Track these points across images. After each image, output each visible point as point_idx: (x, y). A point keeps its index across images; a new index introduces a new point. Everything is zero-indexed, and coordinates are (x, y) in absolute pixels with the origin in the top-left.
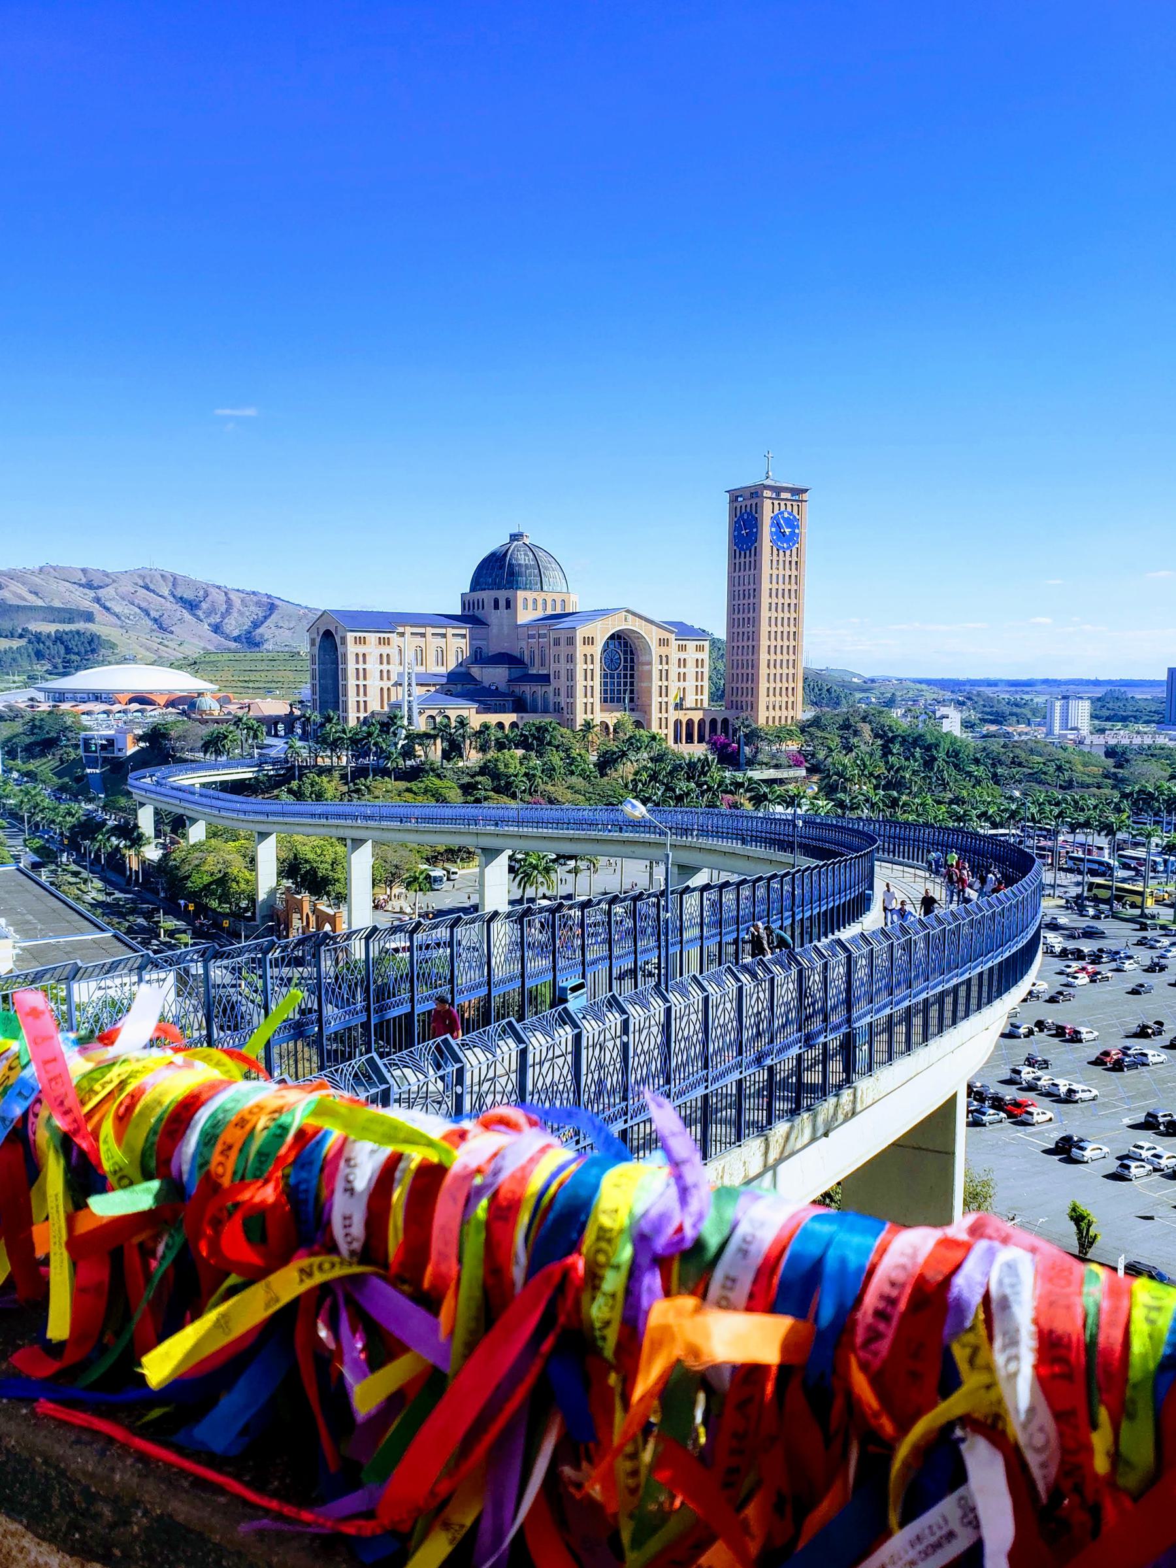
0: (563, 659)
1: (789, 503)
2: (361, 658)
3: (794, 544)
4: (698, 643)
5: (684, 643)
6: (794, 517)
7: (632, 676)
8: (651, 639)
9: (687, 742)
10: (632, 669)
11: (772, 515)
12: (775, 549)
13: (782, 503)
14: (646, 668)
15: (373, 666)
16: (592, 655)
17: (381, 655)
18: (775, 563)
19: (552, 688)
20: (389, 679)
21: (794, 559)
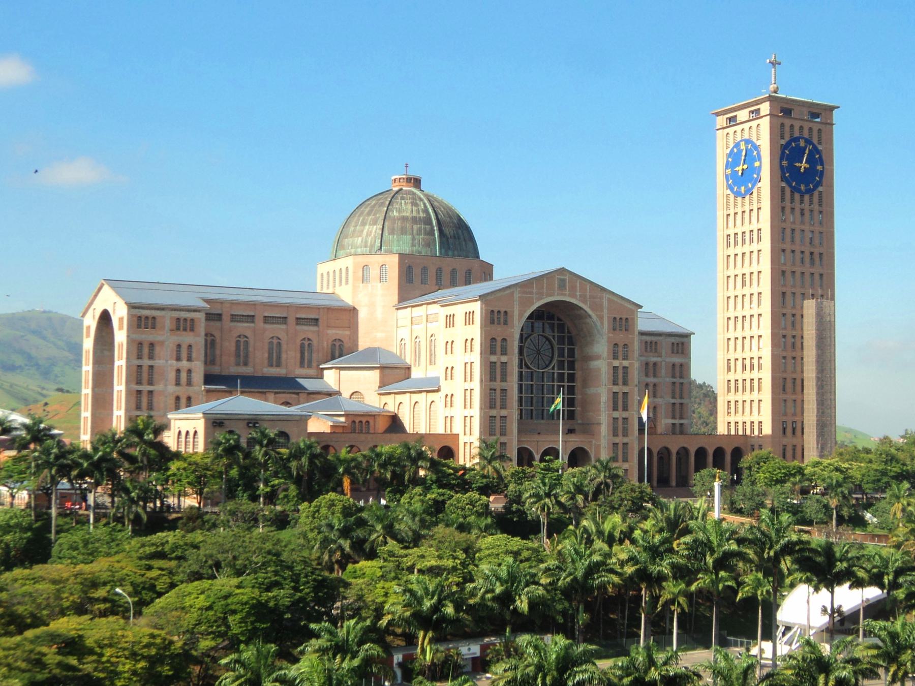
0: (459, 346)
1: (806, 126)
2: (146, 351)
3: (815, 187)
4: (673, 340)
5: (654, 339)
6: (815, 147)
7: (572, 378)
8: (601, 318)
9: (658, 486)
10: (572, 366)
11: (783, 142)
12: (788, 190)
13: (797, 125)
14: (595, 364)
15: (165, 363)
16: (504, 340)
17: (179, 346)
18: (788, 210)
19: (441, 394)
20: (189, 383)
21: (816, 207)
